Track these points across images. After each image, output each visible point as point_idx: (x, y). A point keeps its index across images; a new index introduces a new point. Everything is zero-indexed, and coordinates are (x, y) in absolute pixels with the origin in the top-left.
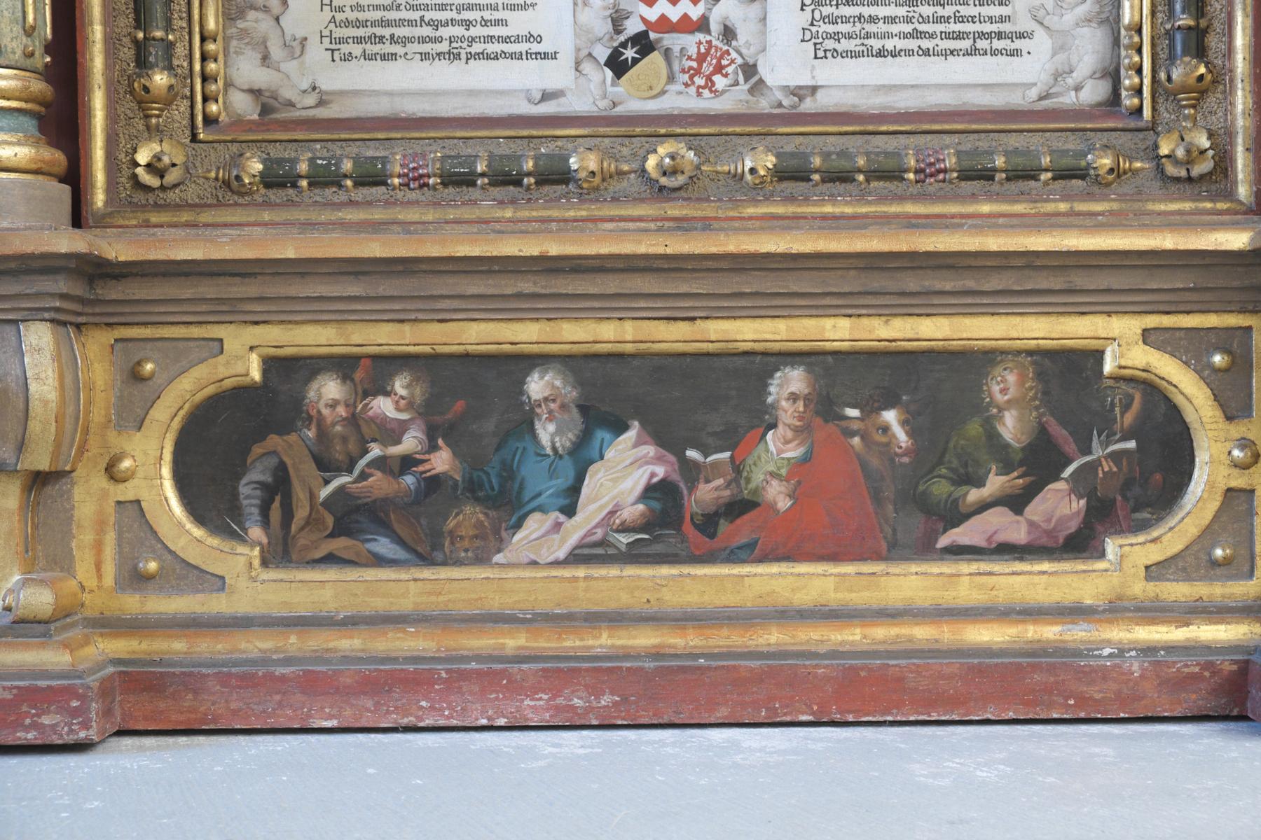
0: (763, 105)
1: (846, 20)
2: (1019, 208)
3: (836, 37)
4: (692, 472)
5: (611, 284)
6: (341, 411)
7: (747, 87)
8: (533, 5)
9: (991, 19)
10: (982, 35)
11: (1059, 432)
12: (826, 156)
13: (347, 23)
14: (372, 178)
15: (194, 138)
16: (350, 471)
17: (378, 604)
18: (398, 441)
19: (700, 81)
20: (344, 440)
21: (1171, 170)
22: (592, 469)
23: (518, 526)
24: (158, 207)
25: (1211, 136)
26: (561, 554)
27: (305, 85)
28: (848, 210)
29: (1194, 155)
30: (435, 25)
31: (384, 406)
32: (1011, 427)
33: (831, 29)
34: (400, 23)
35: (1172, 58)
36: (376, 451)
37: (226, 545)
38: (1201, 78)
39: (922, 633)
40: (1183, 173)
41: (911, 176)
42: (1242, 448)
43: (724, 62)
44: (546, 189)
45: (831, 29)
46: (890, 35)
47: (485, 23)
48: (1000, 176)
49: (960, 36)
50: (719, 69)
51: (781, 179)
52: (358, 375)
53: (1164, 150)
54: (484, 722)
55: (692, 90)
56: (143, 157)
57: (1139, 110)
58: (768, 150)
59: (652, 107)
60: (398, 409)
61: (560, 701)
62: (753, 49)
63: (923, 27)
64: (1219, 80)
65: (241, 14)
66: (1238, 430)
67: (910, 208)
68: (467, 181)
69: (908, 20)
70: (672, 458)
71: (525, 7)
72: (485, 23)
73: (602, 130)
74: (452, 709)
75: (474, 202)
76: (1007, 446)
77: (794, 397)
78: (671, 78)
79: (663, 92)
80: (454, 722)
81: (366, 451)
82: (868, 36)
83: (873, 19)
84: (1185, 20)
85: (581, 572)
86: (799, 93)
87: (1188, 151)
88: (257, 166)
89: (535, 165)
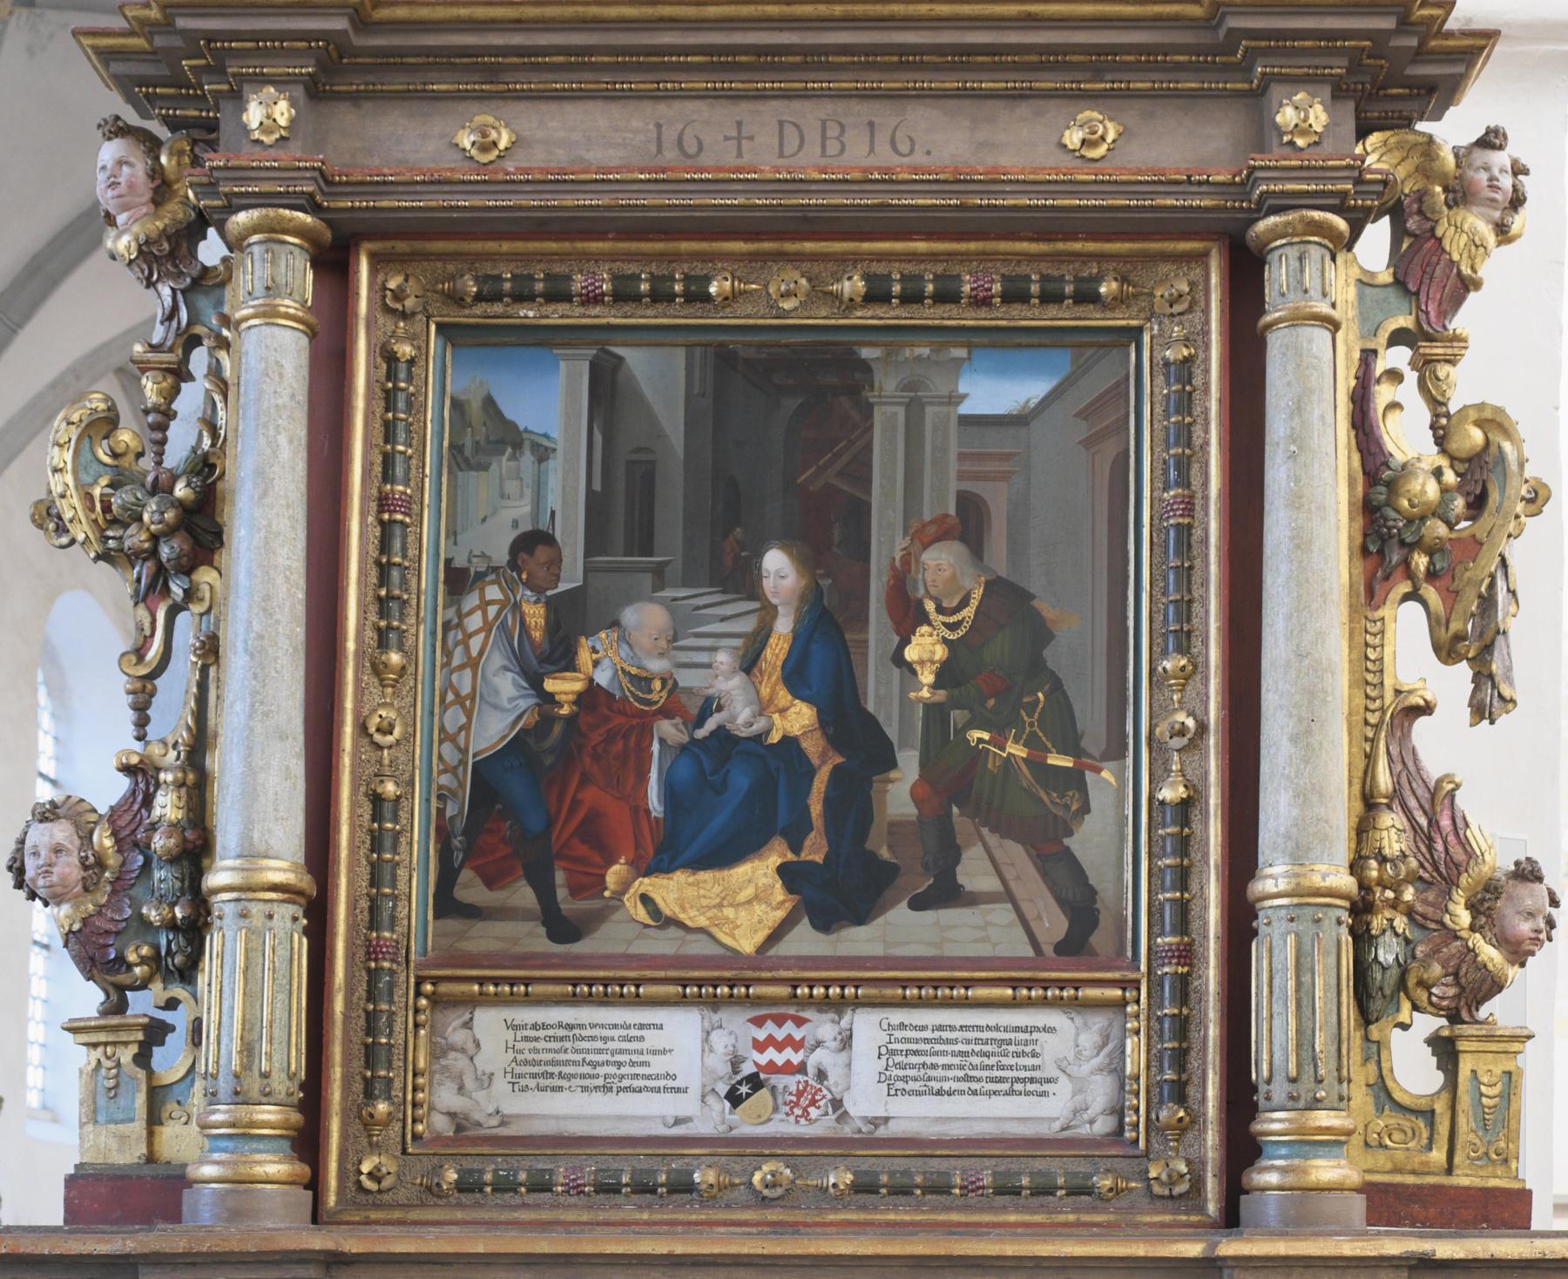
0: (847, 1131)
1: (913, 1067)
2: (1038, 1218)
3: (905, 1079)
7: (834, 1117)
8: (671, 1051)
10: (1018, 1080)
12: (892, 1174)
13: (526, 1063)
14: (541, 1185)
15: (404, 1151)
19: (798, 1111)
21: (1157, 1189)
24: (377, 1206)
25: (1189, 1163)
27: (491, 1110)
28: (907, 1218)
30: (594, 1065)
33: (901, 1073)
34: (567, 1063)
35: (1161, 1102)
38: (1181, 1119)
40: (1167, 1192)
41: (957, 1191)
43: (817, 1097)
44: (675, 1197)
45: (901, 1073)
46: (946, 1079)
47: (633, 1064)
48: (1026, 1192)
49: (1001, 1080)
51: (857, 1192)
53: (1152, 1174)
55: (792, 1118)
56: (366, 1167)
57: (1137, 1140)
58: (848, 1169)
59: (761, 1131)
62: (840, 1088)
64: (1195, 1121)
65: (444, 1054)
67: (955, 1217)
68: (615, 1189)
69: (961, 1067)
71: (664, 1052)
72: (633, 1064)
73: (720, 1150)
75: (618, 1207)
78: (776, 1109)
79: (769, 1120)
82: (929, 1079)
83: (934, 1066)
84: (1169, 1075)
86: (875, 1122)
87: (1170, 1176)
88: (452, 1176)
89: (668, 1178)
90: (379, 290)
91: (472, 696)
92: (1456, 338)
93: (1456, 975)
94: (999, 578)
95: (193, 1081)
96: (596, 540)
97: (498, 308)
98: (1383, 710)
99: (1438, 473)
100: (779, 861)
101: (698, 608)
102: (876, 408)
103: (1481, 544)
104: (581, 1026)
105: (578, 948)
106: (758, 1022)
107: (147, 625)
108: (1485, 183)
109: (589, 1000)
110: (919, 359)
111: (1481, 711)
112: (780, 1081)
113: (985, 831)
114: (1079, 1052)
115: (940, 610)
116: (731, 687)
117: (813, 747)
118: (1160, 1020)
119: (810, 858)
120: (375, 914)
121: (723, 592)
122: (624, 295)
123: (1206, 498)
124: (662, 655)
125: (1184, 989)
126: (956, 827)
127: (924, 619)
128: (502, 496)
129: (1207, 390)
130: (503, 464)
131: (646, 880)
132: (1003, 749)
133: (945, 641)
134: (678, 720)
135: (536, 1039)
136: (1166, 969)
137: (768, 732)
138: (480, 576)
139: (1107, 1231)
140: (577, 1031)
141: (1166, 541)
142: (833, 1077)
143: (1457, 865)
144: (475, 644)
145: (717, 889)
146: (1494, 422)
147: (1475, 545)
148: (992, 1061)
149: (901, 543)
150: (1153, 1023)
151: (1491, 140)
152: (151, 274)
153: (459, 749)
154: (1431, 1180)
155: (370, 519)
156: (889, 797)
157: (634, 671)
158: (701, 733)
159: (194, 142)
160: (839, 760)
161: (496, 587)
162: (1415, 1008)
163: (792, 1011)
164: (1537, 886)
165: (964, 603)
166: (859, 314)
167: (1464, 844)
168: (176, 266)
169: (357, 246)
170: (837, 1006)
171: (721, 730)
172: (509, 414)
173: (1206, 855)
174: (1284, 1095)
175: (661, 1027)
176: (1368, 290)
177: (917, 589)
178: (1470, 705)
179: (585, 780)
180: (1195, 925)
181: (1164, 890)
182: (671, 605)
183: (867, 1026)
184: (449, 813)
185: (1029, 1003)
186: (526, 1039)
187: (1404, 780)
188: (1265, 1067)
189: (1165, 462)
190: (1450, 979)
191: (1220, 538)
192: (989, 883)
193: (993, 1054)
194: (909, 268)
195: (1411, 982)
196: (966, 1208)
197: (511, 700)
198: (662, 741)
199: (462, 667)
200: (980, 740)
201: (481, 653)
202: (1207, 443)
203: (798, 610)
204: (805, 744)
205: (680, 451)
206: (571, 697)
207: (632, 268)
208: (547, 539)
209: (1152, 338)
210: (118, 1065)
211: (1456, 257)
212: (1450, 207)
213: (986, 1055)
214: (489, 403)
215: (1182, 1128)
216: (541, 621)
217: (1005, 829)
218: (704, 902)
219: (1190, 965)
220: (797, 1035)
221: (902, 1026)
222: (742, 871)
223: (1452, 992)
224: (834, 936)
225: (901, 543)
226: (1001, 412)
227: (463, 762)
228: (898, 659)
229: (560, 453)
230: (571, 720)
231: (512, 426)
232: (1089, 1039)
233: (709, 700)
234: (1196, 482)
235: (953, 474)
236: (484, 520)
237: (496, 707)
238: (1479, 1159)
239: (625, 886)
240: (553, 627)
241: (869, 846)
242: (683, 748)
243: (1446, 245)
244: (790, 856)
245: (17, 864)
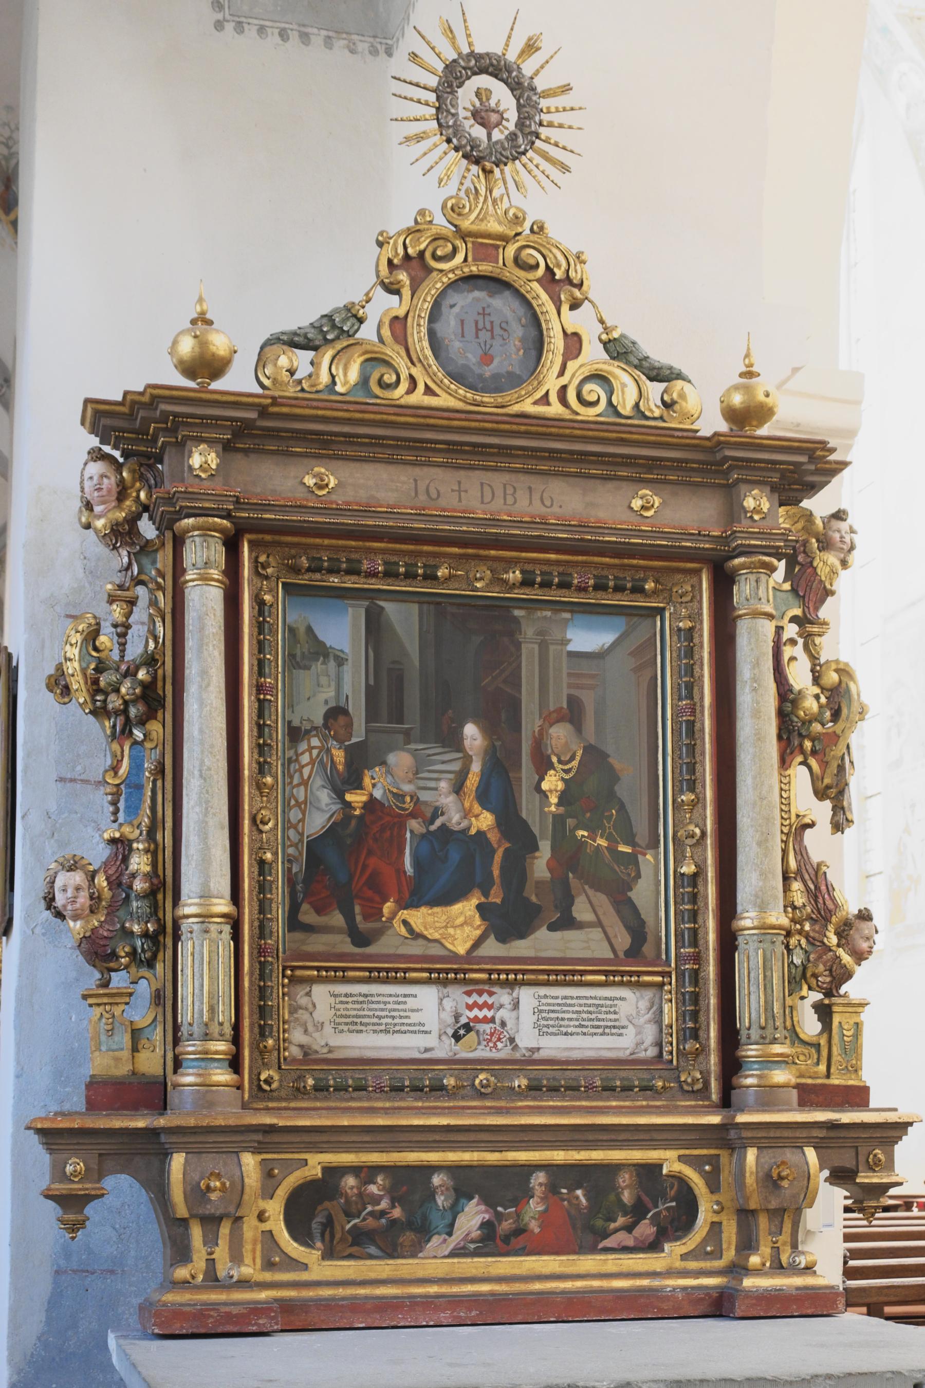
0: (517, 1055)
1: (552, 1019)
2: (627, 1104)
3: (547, 1026)
4: (499, 1217)
5: (472, 1137)
6: (355, 1191)
10: (607, 1027)
11: (646, 1199)
13: (342, 1016)
15: (280, 1068)
16: (359, 1217)
17: (373, 1275)
18: (379, 1204)
19: (491, 1044)
20: (356, 1203)
21: (686, 1088)
22: (459, 1216)
23: (429, 1241)
25: (701, 1073)
26: (446, 1253)
27: (323, 1043)
28: (559, 1104)
29: (695, 1081)
30: (380, 1017)
31: (373, 1189)
32: (627, 1197)
33: (546, 1023)
35: (685, 1040)
36: (369, 1208)
37: (308, 1250)
39: (596, 1283)
41: (583, 1089)
42: (717, 1205)
44: (433, 1093)
45: (546, 1023)
46: (568, 1026)
47: (401, 1017)
49: (598, 1027)
50: (499, 1039)
51: (530, 1090)
52: (362, 1175)
53: (683, 1079)
54: (424, 1323)
55: (488, 1048)
56: (263, 1077)
57: (671, 1061)
58: (525, 1077)
60: (379, 1190)
61: (455, 1314)
63: (583, 1023)
64: (703, 1051)
66: (715, 1197)
67: (584, 1103)
68: (401, 1089)
69: (577, 1020)
70: (491, 1211)
71: (417, 1010)
72: (401, 1017)
74: (411, 1318)
75: (402, 1099)
76: (625, 1205)
77: (541, 1184)
78: (479, 1043)
79: (476, 1049)
80: (412, 1324)
81: (366, 1208)
82: (561, 1026)
83: (563, 1019)
84: (690, 1025)
85: (456, 1260)
86: (533, 1050)
87: (693, 1080)
88: (311, 1082)
90: (255, 562)
91: (305, 802)
92: (825, 623)
93: (831, 971)
94: (591, 745)
95: (156, 1026)
96: (372, 714)
97: (318, 576)
98: (790, 826)
99: (817, 697)
100: (477, 902)
101: (429, 755)
102: (523, 645)
103: (839, 737)
104: (372, 995)
105: (370, 950)
106: (469, 994)
107: (119, 753)
108: (838, 539)
109: (379, 981)
110: (545, 618)
111: (837, 827)
112: (482, 1027)
113: (586, 887)
114: (639, 1012)
115: (560, 762)
116: (448, 801)
117: (493, 837)
118: (683, 994)
120: (262, 931)
121: (443, 747)
122: (391, 574)
123: (702, 706)
124: (410, 782)
125: (696, 977)
126: (572, 885)
127: (551, 766)
128: (318, 685)
129: (702, 647)
130: (318, 666)
131: (405, 912)
132: (595, 841)
133: (563, 779)
134: (420, 820)
135: (347, 1003)
136: (687, 966)
137: (469, 828)
138: (307, 732)
139: (659, 1111)
140: (369, 998)
141: (681, 728)
143: (830, 911)
144: (306, 771)
145: (444, 917)
146: (844, 672)
147: (835, 738)
148: (593, 1016)
149: (538, 723)
150: (680, 996)
151: (839, 516)
152: (116, 543)
153: (298, 832)
154: (819, 1081)
155: (253, 698)
156: (535, 867)
157: (395, 790)
158: (433, 828)
159: (141, 465)
160: (508, 845)
161: (316, 739)
162: (810, 988)
163: (486, 987)
164: (869, 923)
165: (572, 758)
166: (516, 591)
167: (833, 899)
168: (131, 539)
169: (243, 536)
170: (510, 985)
171: (443, 825)
172: (321, 636)
173: (706, 904)
174: (758, 1036)
175: (416, 996)
176: (778, 593)
177: (547, 750)
178: (831, 823)
179: (370, 853)
180: (701, 942)
181: (683, 923)
182: (414, 753)
183: (527, 996)
184: (294, 870)
185: (613, 984)
186: (341, 1002)
187: (802, 864)
188: (747, 1020)
189: (679, 684)
190: (827, 973)
191: (711, 730)
193: (594, 1012)
194: (545, 568)
195: (809, 974)
196: (588, 1098)
197: (327, 805)
198: (412, 832)
199: (298, 785)
200: (583, 836)
201: (309, 777)
202: (703, 676)
203: (484, 759)
204: (489, 836)
205: (417, 663)
206: (360, 805)
207: (394, 559)
208: (343, 711)
210: (113, 1016)
211: (823, 578)
212: (820, 551)
213: (590, 1013)
214: (309, 630)
215: (697, 1053)
216: (343, 760)
217: (597, 887)
218: (438, 925)
219: (699, 964)
220: (490, 1002)
221: (546, 996)
222: (457, 907)
223: (828, 979)
224: (507, 946)
227: (301, 841)
229: (350, 661)
230: (360, 817)
231: (323, 644)
232: (643, 1004)
233: (437, 809)
234: (697, 698)
235: (565, 685)
236: (309, 699)
237: (318, 809)
238: (843, 1070)
239: (394, 915)
240: (349, 763)
241: (525, 894)
242: (423, 836)
243: (819, 571)
244: (483, 899)
245: (51, 896)
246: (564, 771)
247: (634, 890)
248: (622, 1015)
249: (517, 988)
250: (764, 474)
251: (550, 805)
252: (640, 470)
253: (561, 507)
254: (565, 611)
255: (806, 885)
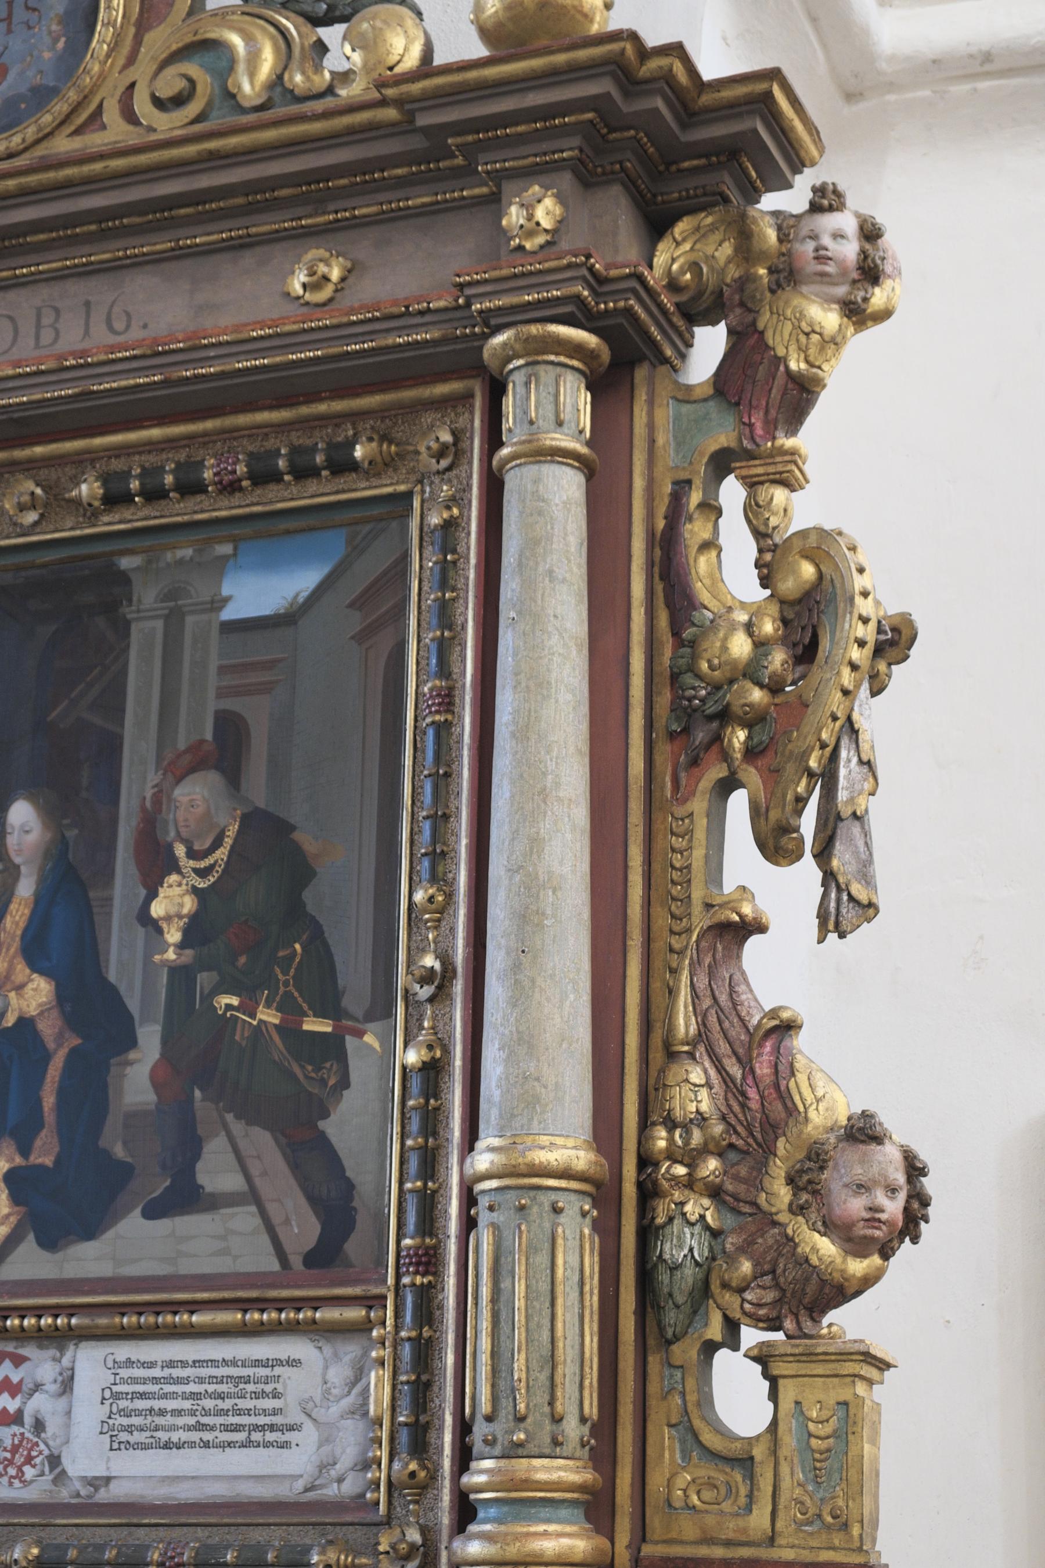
0: (64, 1495)
1: (139, 1413)
3: (129, 1429)
7: (51, 1477)
9: (265, 1412)
10: (257, 1428)
19: (12, 1471)
33: (125, 1421)
43: (34, 1453)
45: (125, 1421)
46: (174, 1428)
49: (237, 1428)
50: (29, 1460)
57: (377, 1503)
62: (58, 1441)
63: (205, 1420)
69: (193, 1413)
82: (156, 1429)
83: (162, 1412)
94: (257, 809)
102: (134, 627)
103: (807, 706)
108: (812, 255)
110: (180, 562)
113: (230, 1117)
114: (328, 1391)
115: (191, 854)
117: (48, 1028)
119: (40, 1160)
126: (199, 1114)
132: (253, 1016)
133: (195, 891)
142: (52, 1428)
143: (774, 1127)
148: (227, 1404)
149: (153, 778)
154: (745, 1552)
160: (76, 1041)
165: (217, 843)
167: (784, 1097)
177: (167, 833)
187: (712, 1019)
192: (231, 1182)
193: (229, 1396)
195: (715, 1287)
200: (229, 1007)
203: (42, 869)
209: (423, 501)
211: (781, 352)
212: (773, 292)
213: (221, 1396)
217: (250, 1115)
220: (15, 1379)
223: (770, 1296)
224: (59, 1255)
225: (153, 778)
226: (267, 612)
228: (144, 918)
232: (339, 1374)
235: (211, 693)
241: (102, 1143)
243: (769, 336)
244: (18, 1160)
246: (196, 871)
247: (333, 1117)
248: (290, 1402)
249: (72, 1347)
250: (544, 146)
251: (164, 947)
252: (299, 211)
253: (145, 326)
254: (221, 540)
255: (720, 1069)
